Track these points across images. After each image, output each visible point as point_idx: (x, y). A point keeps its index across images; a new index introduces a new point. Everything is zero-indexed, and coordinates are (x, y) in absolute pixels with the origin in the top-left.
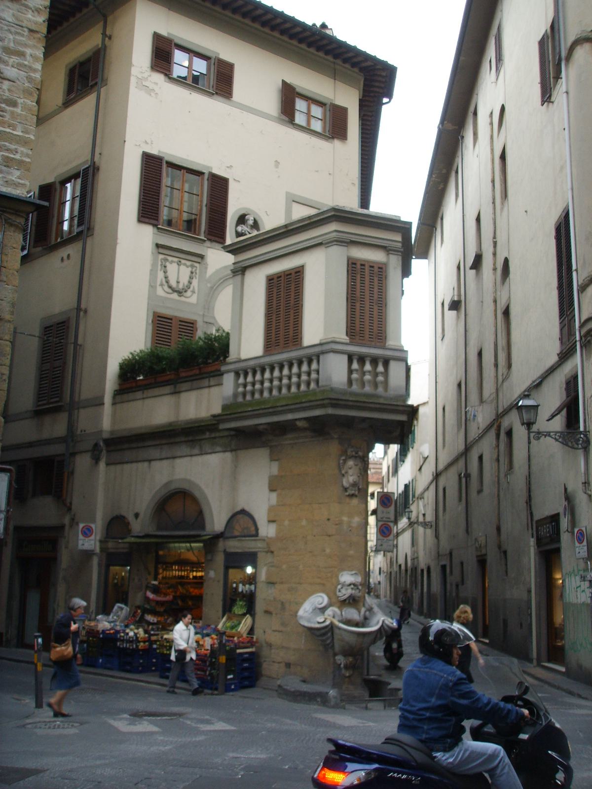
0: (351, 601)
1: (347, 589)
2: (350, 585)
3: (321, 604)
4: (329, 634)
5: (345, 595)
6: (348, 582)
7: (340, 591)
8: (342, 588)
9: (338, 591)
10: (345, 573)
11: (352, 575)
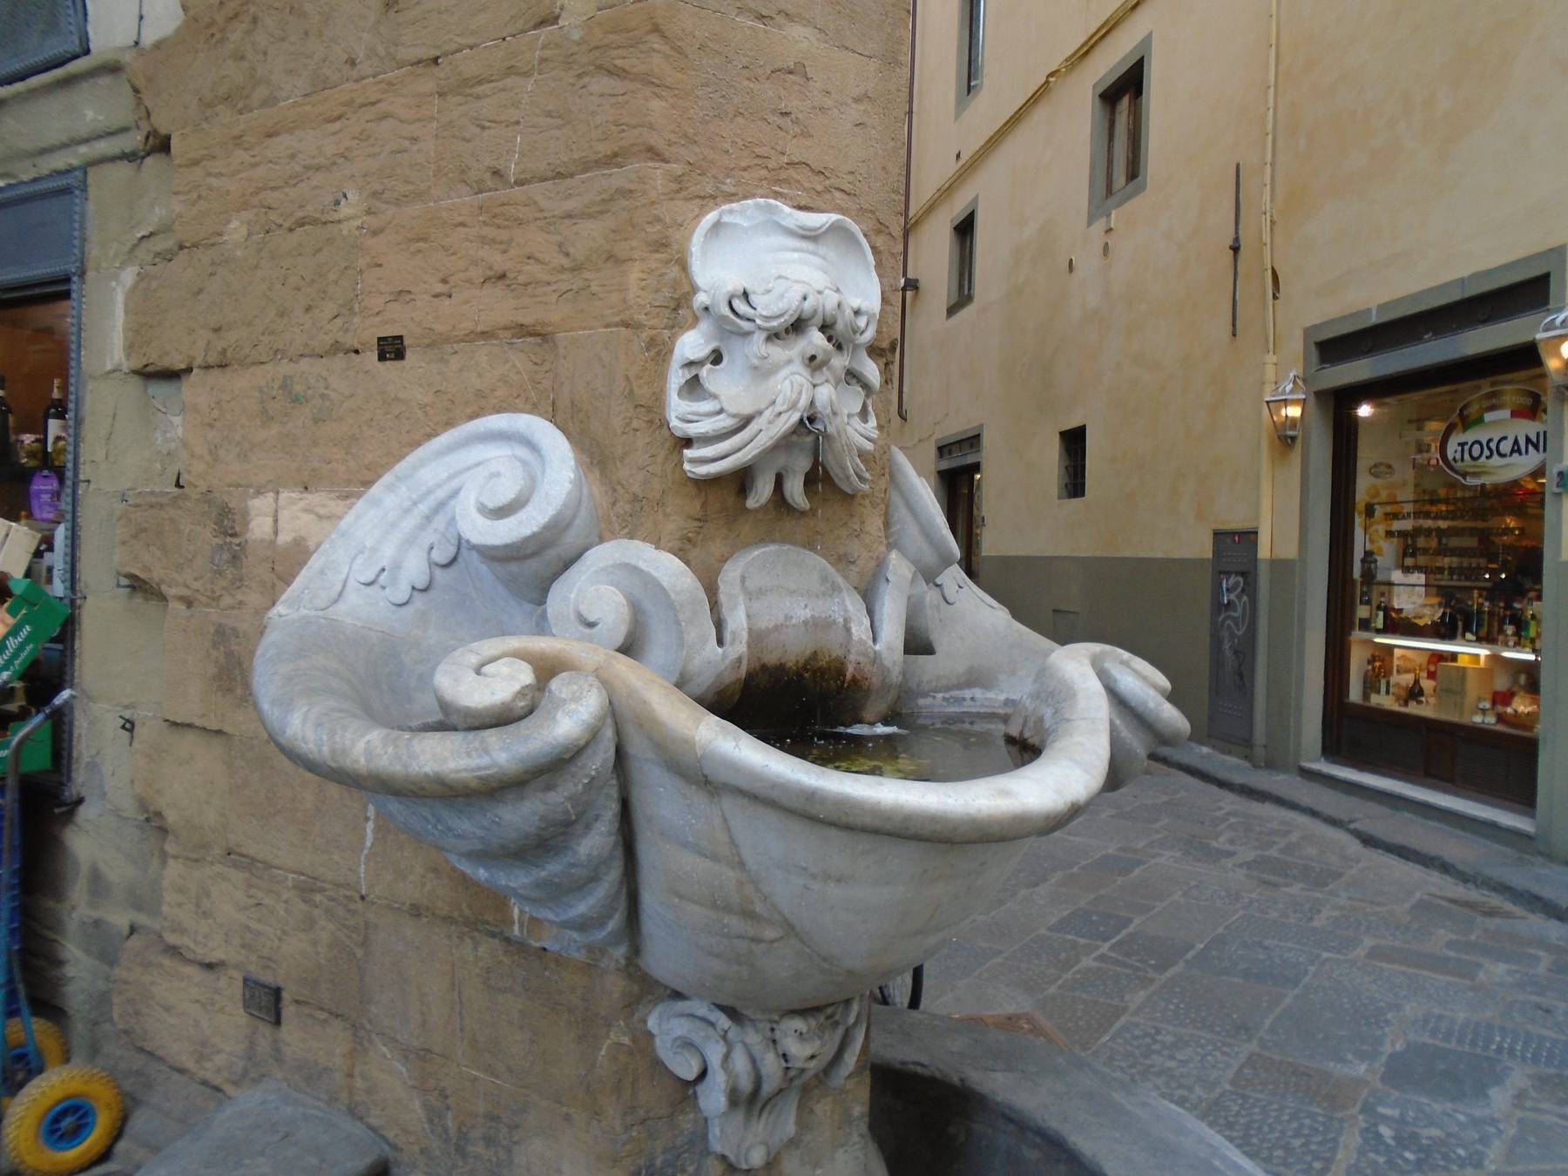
0: (795, 489)
1: (761, 372)
2: (798, 326)
3: (501, 512)
4: (597, 841)
5: (746, 421)
6: (774, 304)
7: (693, 387)
8: (717, 358)
9: (676, 378)
10: (743, 213)
11: (811, 236)
